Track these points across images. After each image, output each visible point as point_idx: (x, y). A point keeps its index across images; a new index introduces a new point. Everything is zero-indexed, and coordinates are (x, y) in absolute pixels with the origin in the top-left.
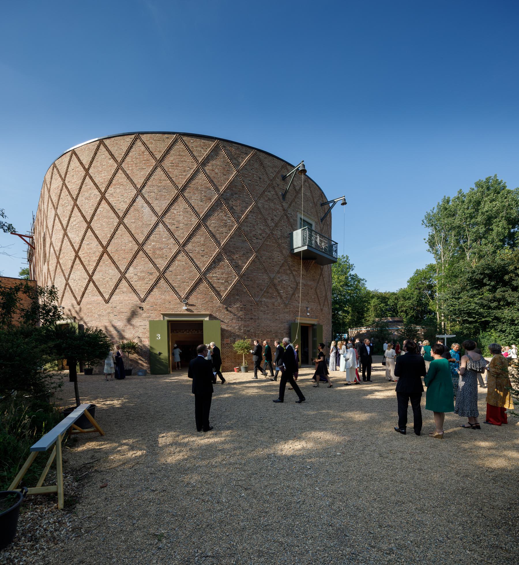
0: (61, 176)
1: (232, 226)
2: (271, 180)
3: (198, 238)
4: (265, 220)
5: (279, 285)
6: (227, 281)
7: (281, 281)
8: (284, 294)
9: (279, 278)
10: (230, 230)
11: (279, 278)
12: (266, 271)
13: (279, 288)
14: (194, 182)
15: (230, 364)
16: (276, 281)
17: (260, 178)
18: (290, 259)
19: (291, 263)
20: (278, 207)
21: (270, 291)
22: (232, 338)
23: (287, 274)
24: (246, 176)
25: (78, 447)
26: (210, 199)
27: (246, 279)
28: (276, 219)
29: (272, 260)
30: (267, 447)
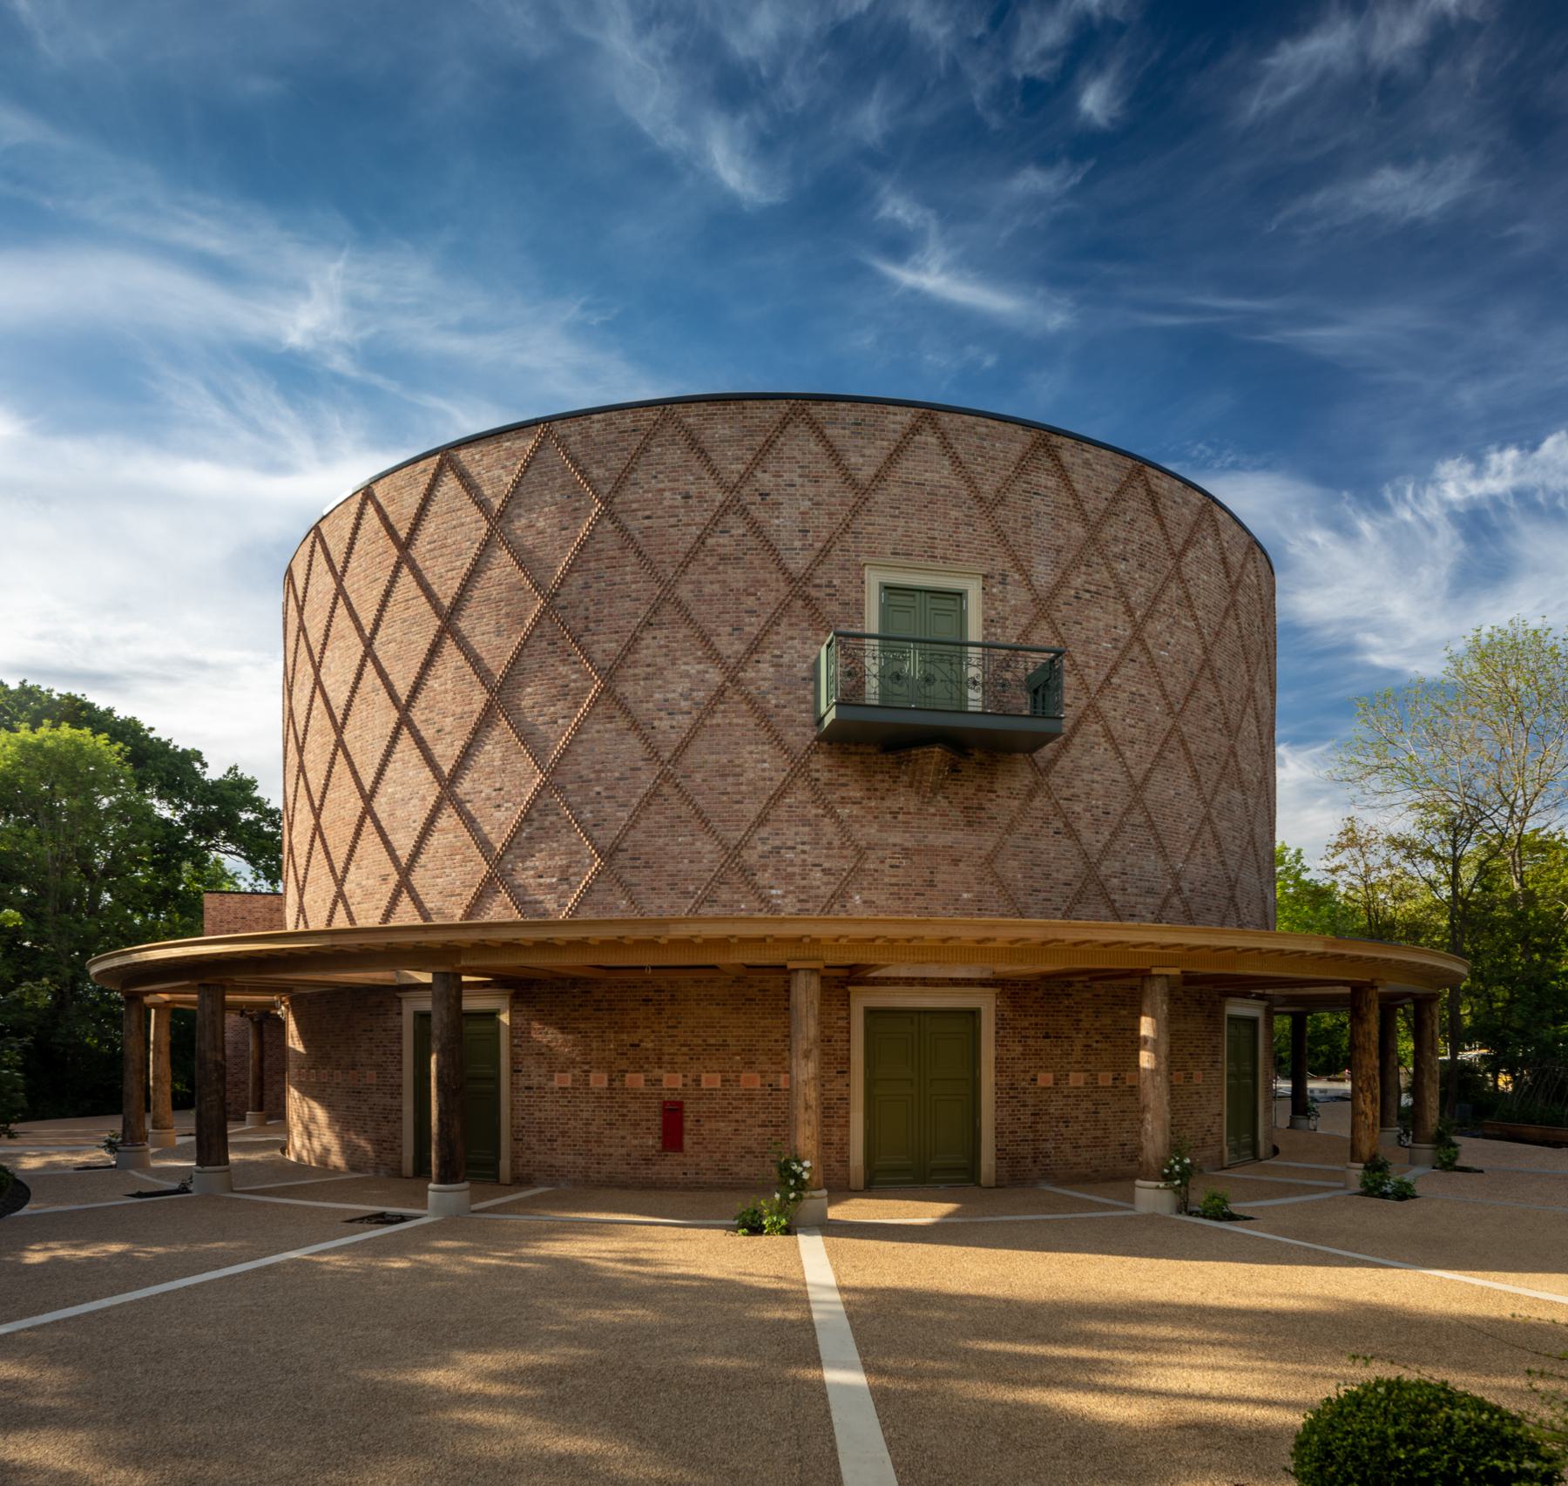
0: (359, 628)
1: (586, 690)
2: (733, 489)
3: (492, 751)
4: (706, 640)
5: (764, 868)
6: (564, 879)
7: (777, 850)
8: (790, 899)
9: (763, 840)
10: (577, 705)
11: (763, 840)
12: (706, 822)
13: (763, 878)
14: (482, 582)
15: (570, 1158)
16: (750, 857)
17: (687, 497)
18: (819, 763)
19: (825, 776)
20: (762, 575)
21: (724, 894)
22: (576, 1071)
23: (805, 822)
24: (635, 506)
25: (425, 1366)
26: (521, 621)
27: (627, 863)
28: (753, 626)
29: (730, 780)
30: (51, 1409)
